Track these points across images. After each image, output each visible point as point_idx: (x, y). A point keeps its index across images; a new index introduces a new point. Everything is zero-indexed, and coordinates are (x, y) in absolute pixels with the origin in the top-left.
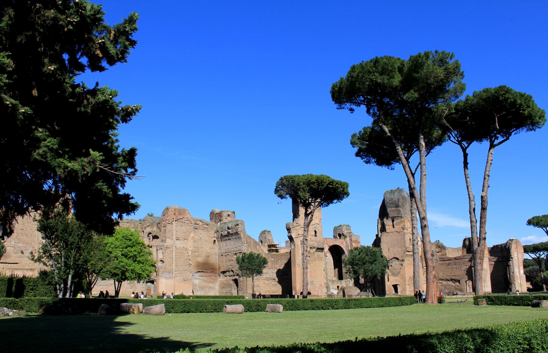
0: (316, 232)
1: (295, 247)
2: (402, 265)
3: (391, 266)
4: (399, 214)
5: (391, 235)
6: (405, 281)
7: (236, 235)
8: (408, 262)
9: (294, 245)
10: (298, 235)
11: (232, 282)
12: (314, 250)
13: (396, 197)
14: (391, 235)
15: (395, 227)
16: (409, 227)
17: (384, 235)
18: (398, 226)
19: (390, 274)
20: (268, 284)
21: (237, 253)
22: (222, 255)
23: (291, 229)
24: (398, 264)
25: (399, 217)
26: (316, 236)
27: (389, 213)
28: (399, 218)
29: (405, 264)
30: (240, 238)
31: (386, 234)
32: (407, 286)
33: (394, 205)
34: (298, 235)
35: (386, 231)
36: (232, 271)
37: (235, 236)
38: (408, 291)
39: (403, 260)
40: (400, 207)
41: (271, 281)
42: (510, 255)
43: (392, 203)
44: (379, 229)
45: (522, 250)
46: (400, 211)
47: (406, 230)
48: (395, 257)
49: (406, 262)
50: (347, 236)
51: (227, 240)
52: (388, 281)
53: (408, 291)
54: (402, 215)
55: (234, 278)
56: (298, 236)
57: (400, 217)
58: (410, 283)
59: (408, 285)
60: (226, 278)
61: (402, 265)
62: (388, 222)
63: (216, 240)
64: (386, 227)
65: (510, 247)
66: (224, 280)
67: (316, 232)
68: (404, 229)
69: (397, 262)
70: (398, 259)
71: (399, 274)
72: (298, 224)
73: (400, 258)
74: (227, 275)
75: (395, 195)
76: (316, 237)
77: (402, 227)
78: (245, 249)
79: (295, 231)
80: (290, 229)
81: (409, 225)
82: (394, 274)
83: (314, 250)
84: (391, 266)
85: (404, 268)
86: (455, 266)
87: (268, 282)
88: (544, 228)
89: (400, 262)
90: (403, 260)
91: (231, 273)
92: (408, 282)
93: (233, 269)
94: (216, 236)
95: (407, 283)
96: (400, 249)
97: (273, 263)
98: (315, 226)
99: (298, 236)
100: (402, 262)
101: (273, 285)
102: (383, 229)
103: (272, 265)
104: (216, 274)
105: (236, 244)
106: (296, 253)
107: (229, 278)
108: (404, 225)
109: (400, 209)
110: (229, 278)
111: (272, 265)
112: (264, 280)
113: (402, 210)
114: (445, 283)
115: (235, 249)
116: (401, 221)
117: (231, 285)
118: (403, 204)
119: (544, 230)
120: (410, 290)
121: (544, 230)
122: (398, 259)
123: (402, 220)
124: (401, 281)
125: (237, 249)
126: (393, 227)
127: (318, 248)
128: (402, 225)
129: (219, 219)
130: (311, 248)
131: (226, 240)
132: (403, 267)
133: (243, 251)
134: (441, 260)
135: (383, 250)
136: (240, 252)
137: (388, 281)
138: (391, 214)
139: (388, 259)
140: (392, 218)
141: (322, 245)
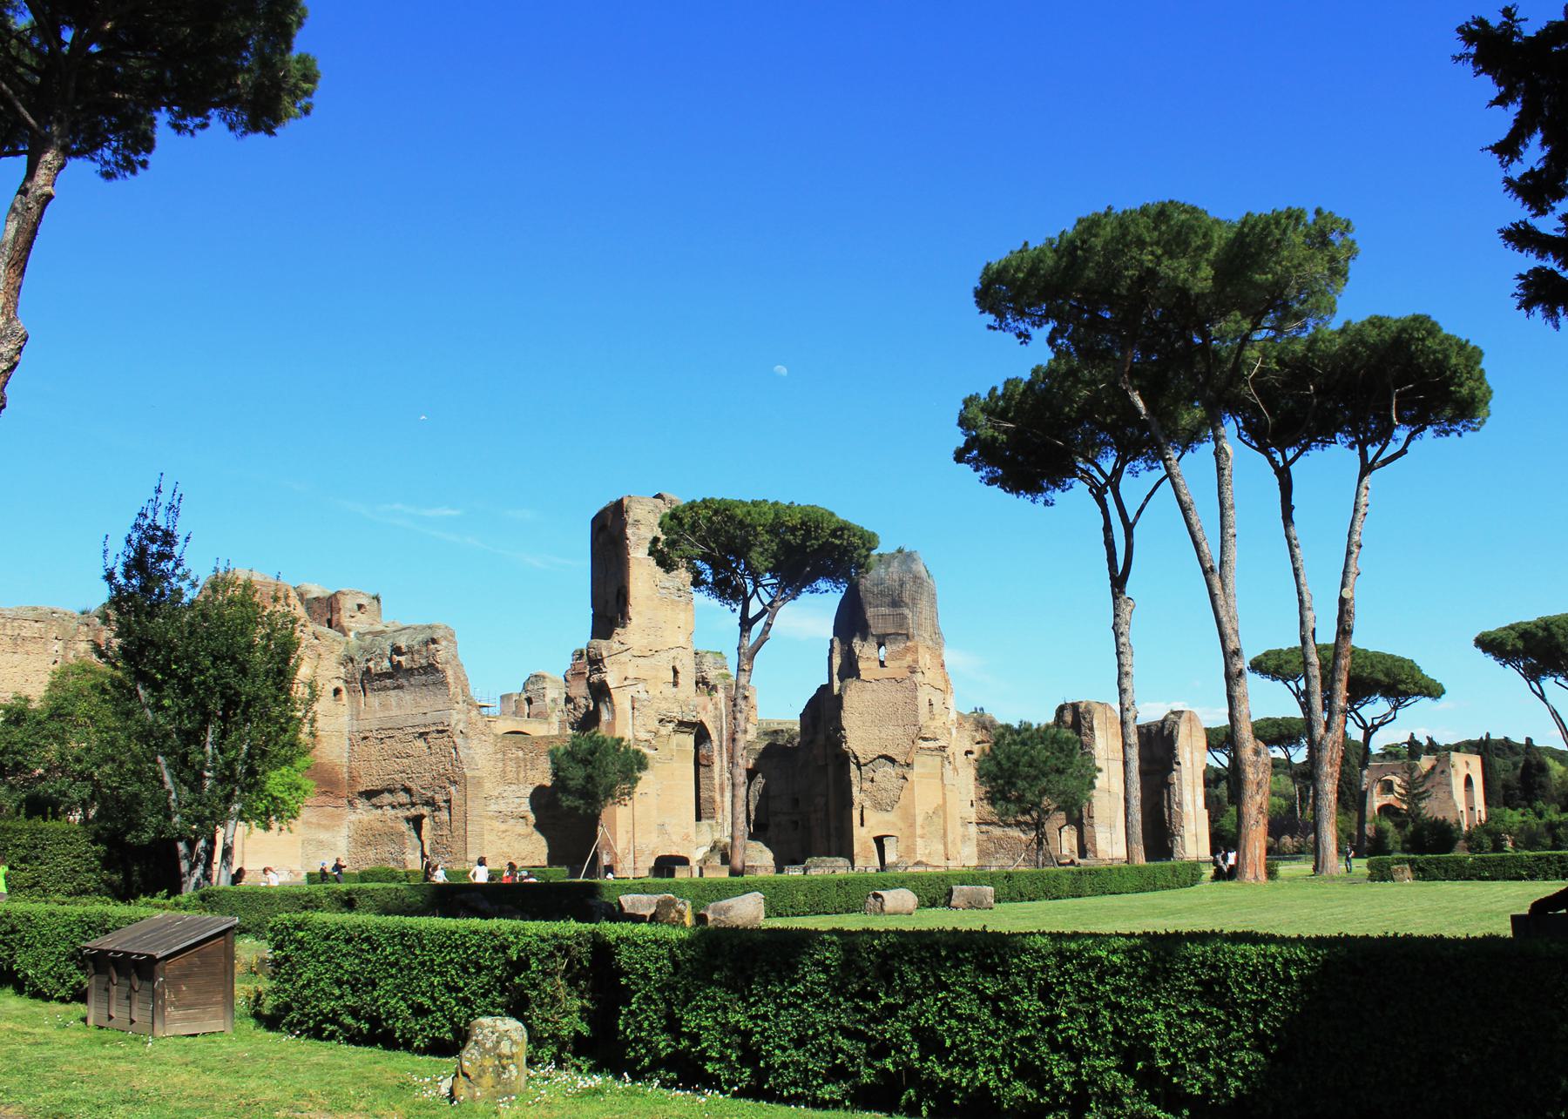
0: (675, 672)
1: (614, 718)
2: (904, 778)
3: (872, 781)
4: (901, 626)
5: (875, 687)
6: (912, 825)
7: (426, 673)
8: (922, 770)
9: (613, 712)
10: (625, 679)
11: (404, 827)
12: (671, 726)
13: (895, 577)
14: (875, 687)
16: (928, 666)
17: (853, 686)
18: (897, 664)
19: (867, 804)
20: (504, 832)
21: (427, 733)
22: (365, 738)
23: (605, 661)
24: (894, 774)
25: (901, 634)
26: (675, 684)
27: (871, 622)
28: (900, 638)
29: (913, 775)
30: (443, 683)
31: (859, 684)
32: (919, 842)
33: (887, 600)
34: (625, 679)
35: (858, 677)
36: (407, 790)
37: (424, 677)
39: (908, 765)
40: (906, 605)
41: (512, 822)
42: (1175, 756)
43: (881, 593)
44: (835, 670)
45: (1203, 743)
46: (904, 617)
47: (920, 675)
49: (917, 768)
50: (719, 686)
51: (389, 689)
52: (862, 825)
54: (911, 630)
55: (414, 812)
56: (626, 683)
57: (904, 637)
58: (925, 831)
60: (379, 811)
61: (904, 778)
62: (866, 652)
63: (344, 690)
64: (861, 665)
65: (1175, 733)
66: (372, 817)
67: (675, 672)
68: (913, 672)
69: (888, 768)
70: (892, 760)
72: (626, 647)
73: (901, 759)
74: (385, 801)
75: (890, 570)
76: (675, 690)
77: (909, 667)
78: (459, 721)
79: (615, 668)
80: (602, 660)
82: (879, 806)
83: (671, 726)
84: (872, 781)
85: (912, 789)
87: (503, 827)
88: (1290, 683)
89: (899, 770)
90: (908, 765)
91: (403, 798)
93: (408, 783)
94: (342, 676)
95: (919, 831)
96: (900, 731)
97: (522, 764)
98: (673, 653)
99: (626, 683)
100: (905, 770)
101: (520, 835)
102: (850, 669)
103: (518, 773)
104: (340, 801)
105: (424, 702)
107: (393, 812)
108: (916, 661)
109: (906, 611)
110: (390, 812)
111: (518, 773)
112: (491, 818)
113: (910, 616)
115: (419, 720)
116: (907, 649)
117: (402, 834)
118: (914, 599)
119: (1289, 687)
120: (927, 852)
121: (1289, 687)
122: (892, 760)
123: (909, 644)
124: (901, 824)
125: (429, 719)
127: (681, 723)
128: (909, 659)
129: (325, 619)
130: (661, 721)
131: (385, 688)
132: (906, 785)
133: (453, 725)
135: (848, 731)
136: (440, 728)
137: (862, 825)
138: (877, 627)
139: (862, 761)
140: (878, 636)
141: (694, 713)
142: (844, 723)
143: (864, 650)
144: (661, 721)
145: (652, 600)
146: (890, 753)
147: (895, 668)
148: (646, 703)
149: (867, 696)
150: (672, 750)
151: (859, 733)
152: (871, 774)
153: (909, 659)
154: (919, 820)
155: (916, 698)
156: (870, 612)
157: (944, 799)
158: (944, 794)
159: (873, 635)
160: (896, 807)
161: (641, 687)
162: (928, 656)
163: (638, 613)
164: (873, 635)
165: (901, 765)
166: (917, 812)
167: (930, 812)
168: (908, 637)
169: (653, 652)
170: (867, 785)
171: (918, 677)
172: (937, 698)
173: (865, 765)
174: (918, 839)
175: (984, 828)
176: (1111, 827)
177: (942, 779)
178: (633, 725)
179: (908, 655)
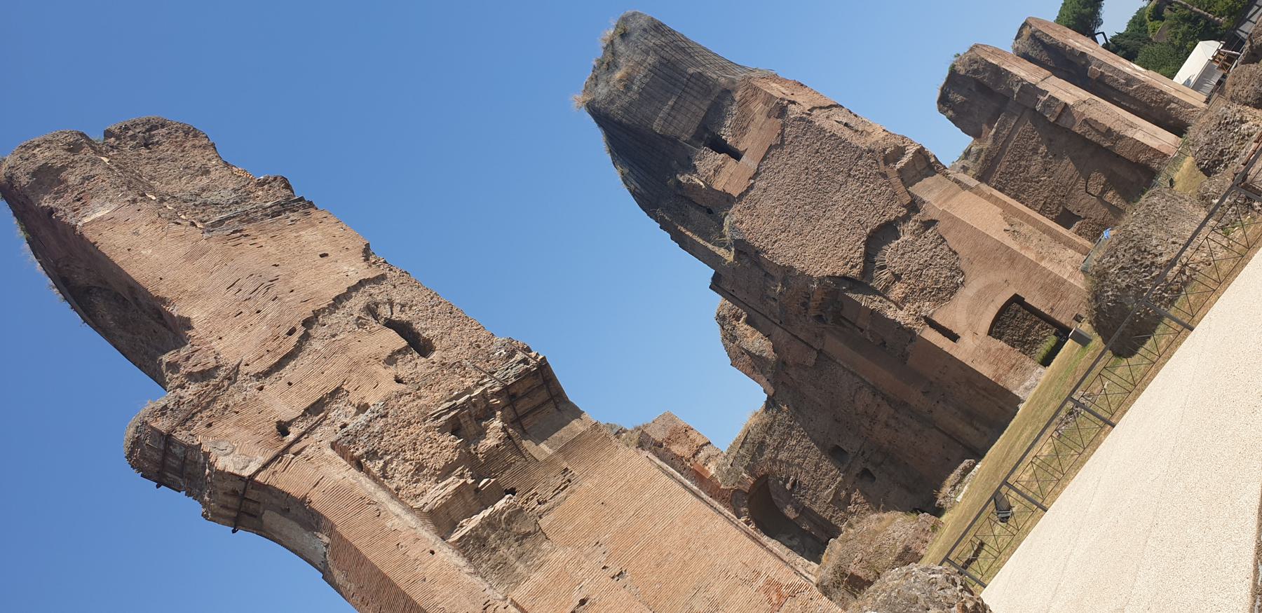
6: (1013, 258)
10: (283, 429)
14: (763, 184)
15: (741, 148)
18: (753, 131)
19: (927, 308)
26: (418, 344)
35: (728, 200)
47: (791, 107)
52: (954, 337)
54: (722, 80)
56: (291, 437)
61: (930, 224)
64: (719, 185)
73: (895, 211)
81: (783, 89)
82: (946, 292)
84: (897, 277)
89: (911, 225)
98: (358, 302)
99: (291, 437)
106: (374, 556)
116: (744, 103)
126: (737, 155)
128: (758, 108)
132: (940, 227)
135: (797, 265)
137: (954, 337)
138: (684, 127)
142: (780, 261)
143: (701, 169)
144: (454, 428)
145: (204, 253)
146: (874, 222)
147: (752, 143)
148: (377, 426)
150: (549, 462)
152: (886, 275)
153: (758, 108)
156: (657, 126)
160: (963, 264)
161: (340, 413)
162: (774, 85)
163: (194, 296)
167: (1008, 227)
169: (300, 331)
170: (897, 291)
176: (1132, 126)
178: (395, 494)
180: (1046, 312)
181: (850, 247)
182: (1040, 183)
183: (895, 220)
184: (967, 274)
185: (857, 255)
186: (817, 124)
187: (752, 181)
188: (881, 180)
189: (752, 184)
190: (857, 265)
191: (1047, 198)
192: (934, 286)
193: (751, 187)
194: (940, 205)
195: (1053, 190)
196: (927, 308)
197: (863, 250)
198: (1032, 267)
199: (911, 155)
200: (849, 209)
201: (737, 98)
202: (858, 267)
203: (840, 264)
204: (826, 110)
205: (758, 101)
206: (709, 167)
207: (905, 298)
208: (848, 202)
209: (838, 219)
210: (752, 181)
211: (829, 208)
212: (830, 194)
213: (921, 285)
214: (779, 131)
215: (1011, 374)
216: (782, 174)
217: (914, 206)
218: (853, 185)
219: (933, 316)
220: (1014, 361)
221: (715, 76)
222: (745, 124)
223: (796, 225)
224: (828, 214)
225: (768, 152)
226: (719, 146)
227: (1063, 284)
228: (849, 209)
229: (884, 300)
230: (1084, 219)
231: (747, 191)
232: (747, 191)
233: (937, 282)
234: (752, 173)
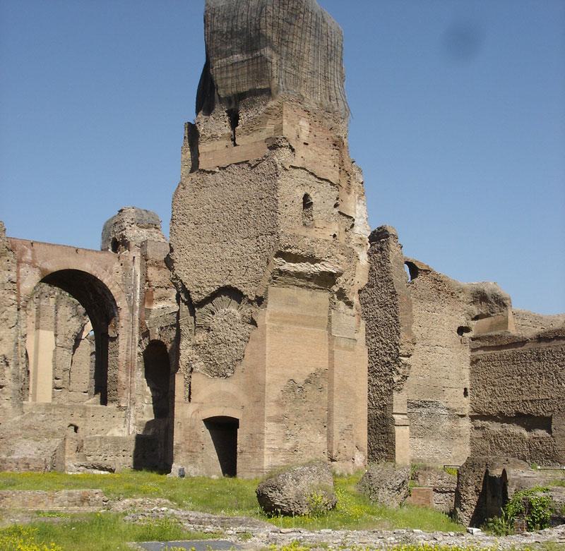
6: (259, 401)
14: (220, 179)
16: (304, 138)
18: (254, 137)
19: (199, 366)
24: (239, 316)
29: (265, 316)
32: (270, 428)
38: (275, 452)
40: (268, 42)
47: (288, 151)
48: (228, 283)
49: (272, 306)
53: (275, 452)
59: (278, 420)
61: (253, 323)
68: (274, 147)
71: (239, 368)
73: (250, 291)
82: (217, 370)
85: (263, 340)
86: (538, 363)
89: (247, 310)
92: (279, 403)
95: (271, 410)
108: (279, 129)
109: (267, 52)
114: (495, 427)
120: (288, 445)
122: (234, 294)
123: (271, 104)
124: (243, 399)
132: (256, 333)
134: (487, 344)
139: (195, 297)
146: (236, 283)
147: (250, 145)
149: (207, 195)
151: (192, 254)
154: (273, 392)
155: (275, 189)
157: (331, 359)
158: (332, 352)
159: (221, 100)
164: (221, 100)
165: (250, 302)
166: (268, 378)
167: (300, 381)
168: (268, 93)
171: (283, 156)
172: (322, 197)
173: (201, 304)
174: (267, 424)
175: (479, 423)
177: (329, 328)
179: (270, 121)
180: (238, 449)
181: (211, 280)
182: (559, 386)
183: (245, 296)
184: (236, 373)
185: (208, 289)
186: (279, 181)
187: (217, 170)
188: (264, 263)
189: (215, 172)
190: (201, 295)
191: (552, 398)
192: (215, 359)
193: (213, 173)
194: (269, 320)
195: (559, 398)
196: (199, 366)
197: (213, 290)
198: (259, 418)
199: (316, 270)
200: (235, 257)
201: (269, 105)
202: (200, 296)
203: (195, 283)
204: (317, 180)
205: (274, 123)
206: (213, 129)
207: (197, 345)
208: (240, 253)
209: (227, 255)
210: (217, 170)
211: (229, 243)
212: (238, 235)
213: (211, 350)
214: (260, 158)
215: (184, 454)
216: (234, 187)
217: (260, 301)
218: (251, 245)
219: (195, 374)
220: (194, 450)
221: (275, 74)
222: (255, 128)
223: (205, 228)
224: (224, 245)
225: (242, 163)
226: (234, 122)
227: (260, 448)
228: (235, 257)
229: (193, 333)
230: (552, 436)
231: (208, 172)
232: (208, 172)
233: (220, 359)
234: (222, 165)
